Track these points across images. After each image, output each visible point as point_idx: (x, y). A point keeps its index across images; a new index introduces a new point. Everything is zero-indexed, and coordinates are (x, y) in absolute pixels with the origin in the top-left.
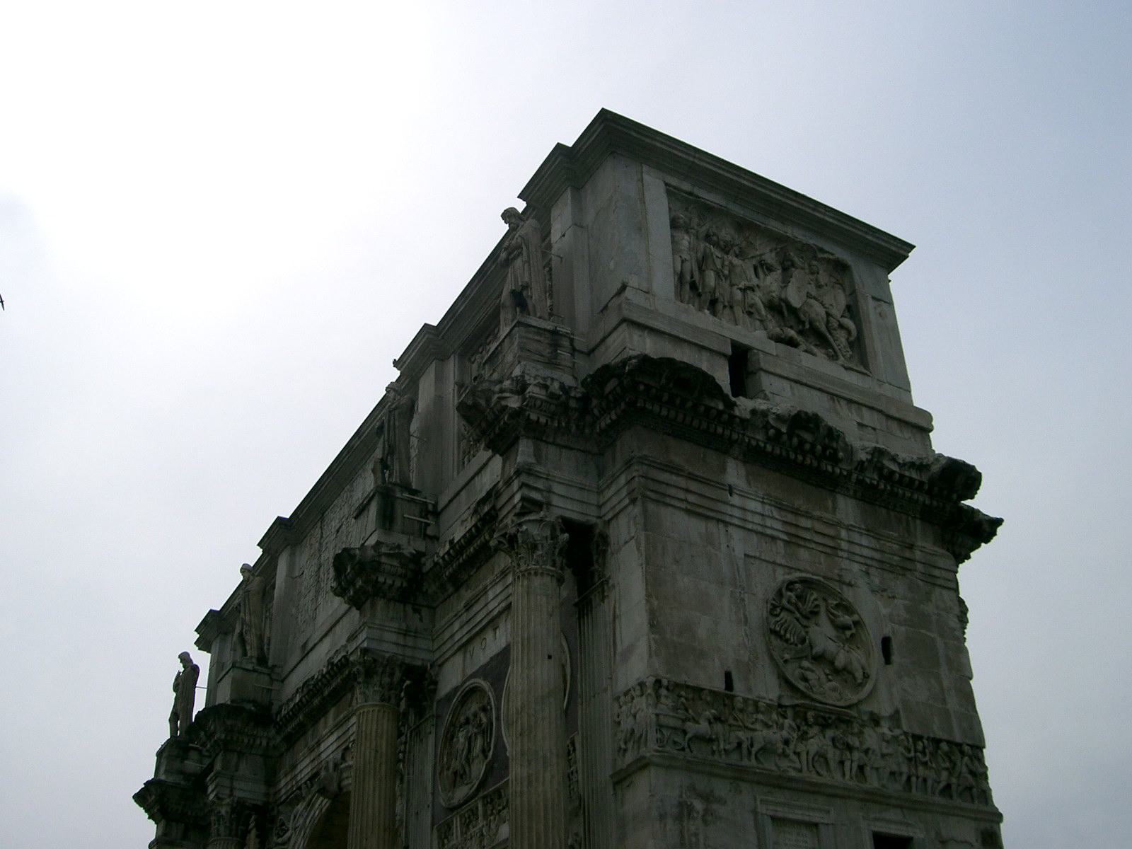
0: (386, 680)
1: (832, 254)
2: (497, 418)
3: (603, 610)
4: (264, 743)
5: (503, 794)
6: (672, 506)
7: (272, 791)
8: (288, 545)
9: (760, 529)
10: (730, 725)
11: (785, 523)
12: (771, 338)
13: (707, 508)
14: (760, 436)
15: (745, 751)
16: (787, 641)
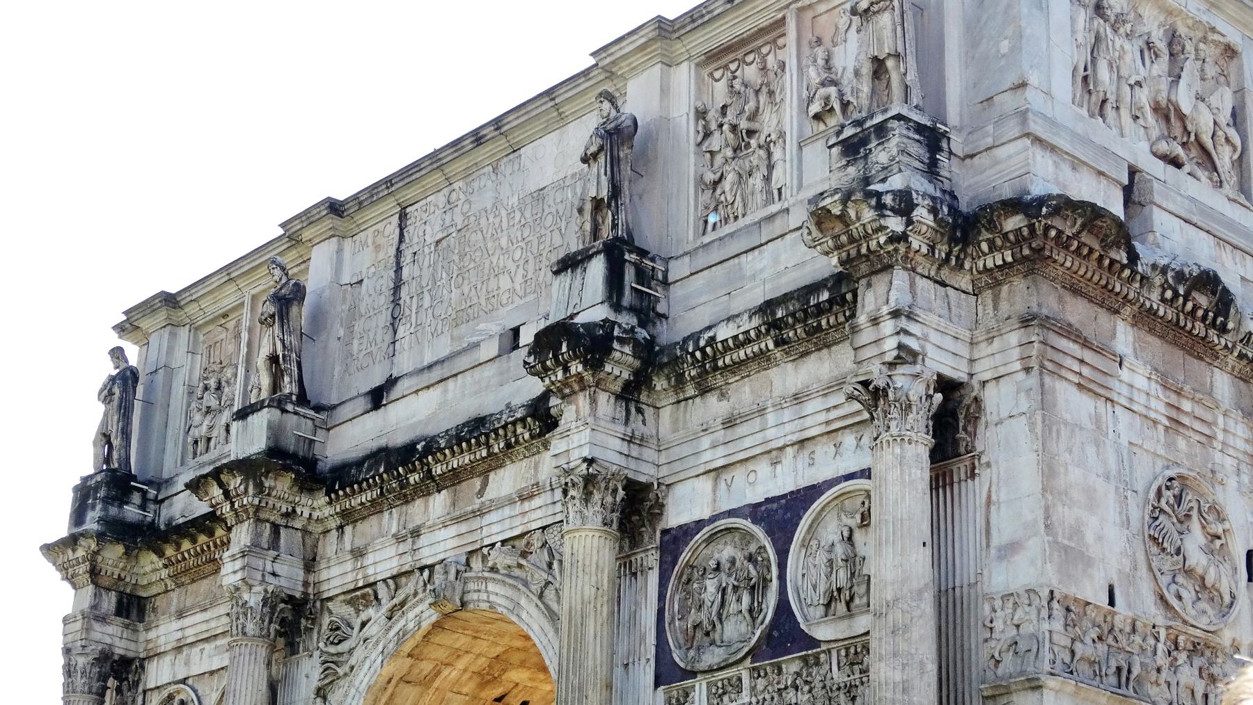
0: (609, 499)
1: (1223, 35)
2: (867, 237)
3: (973, 493)
4: (306, 515)
5: (784, 670)
6: (1066, 379)
7: (311, 579)
8: (333, 236)
9: (1144, 411)
10: (1109, 646)
11: (1168, 404)
12: (1155, 154)
13: (1099, 384)
14: (1155, 296)
15: (1124, 679)
16: (1164, 550)
